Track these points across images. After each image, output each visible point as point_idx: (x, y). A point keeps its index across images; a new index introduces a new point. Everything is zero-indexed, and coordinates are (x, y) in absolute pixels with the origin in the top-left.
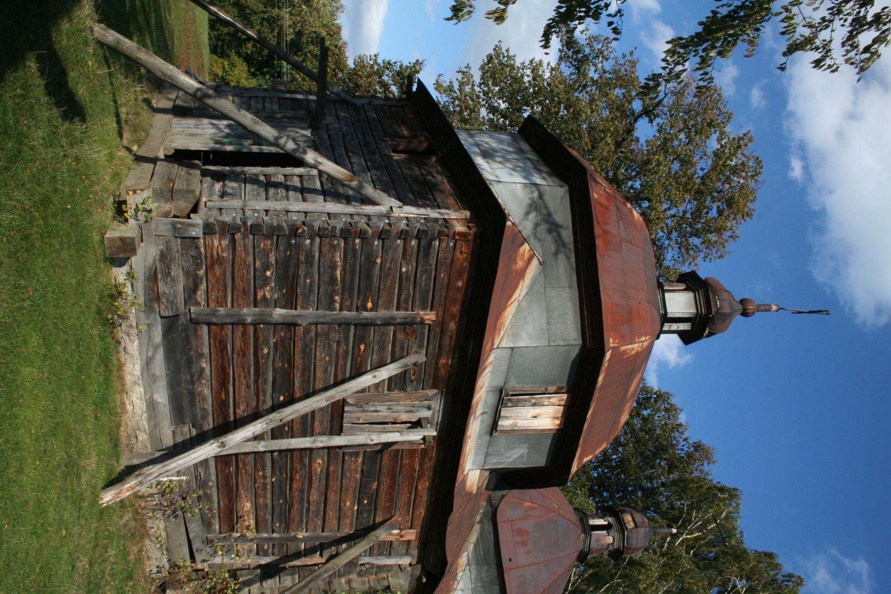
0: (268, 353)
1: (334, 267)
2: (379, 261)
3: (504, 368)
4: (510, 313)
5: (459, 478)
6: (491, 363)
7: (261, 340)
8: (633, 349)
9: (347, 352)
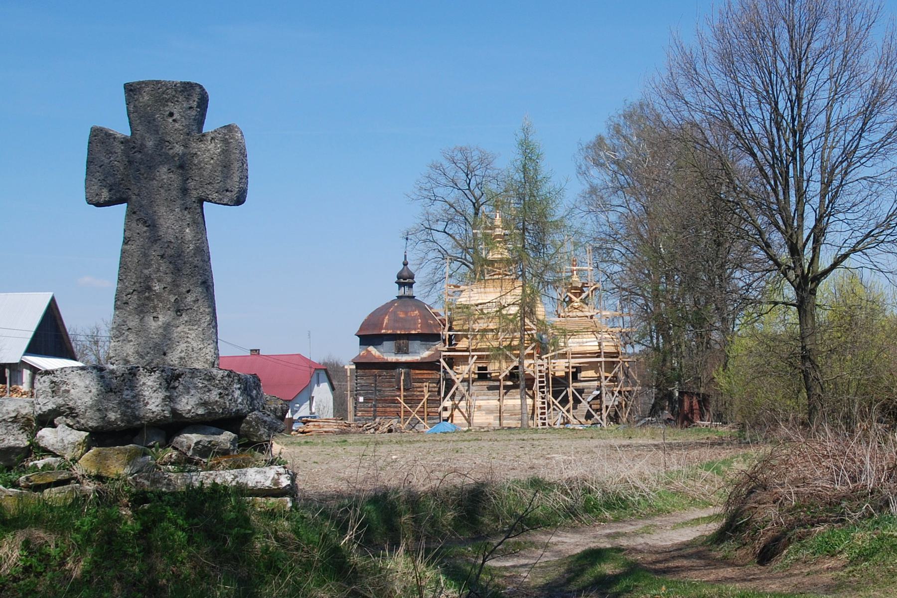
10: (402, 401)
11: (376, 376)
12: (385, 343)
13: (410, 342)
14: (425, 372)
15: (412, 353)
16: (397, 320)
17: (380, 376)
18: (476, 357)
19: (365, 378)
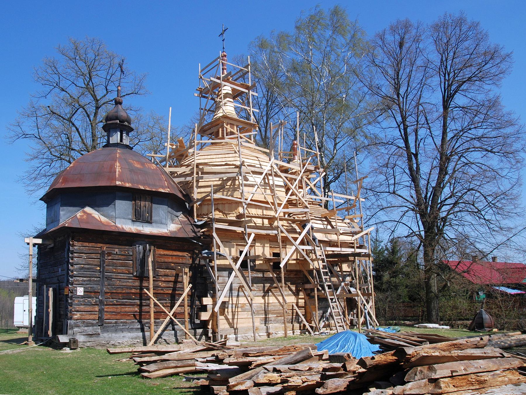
0: (116, 301)
1: (85, 281)
2: (82, 266)
3: (124, 220)
4: (103, 219)
5: (169, 235)
6: (122, 226)
7: (111, 303)
8: (119, 171)
9: (116, 275)
10: (151, 295)
11: (103, 254)
12: (118, 202)
13: (154, 206)
14: (175, 253)
15: (156, 222)
16: (133, 170)
17: (109, 254)
18: (253, 236)
19: (84, 256)
